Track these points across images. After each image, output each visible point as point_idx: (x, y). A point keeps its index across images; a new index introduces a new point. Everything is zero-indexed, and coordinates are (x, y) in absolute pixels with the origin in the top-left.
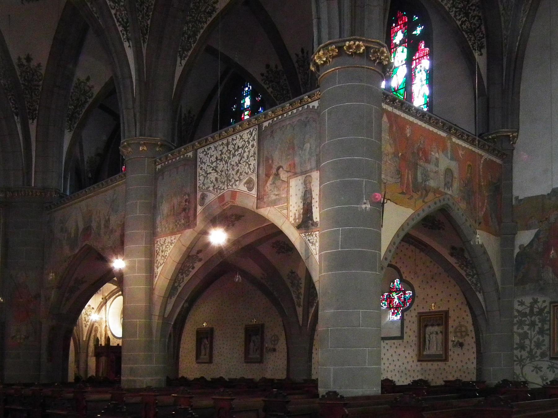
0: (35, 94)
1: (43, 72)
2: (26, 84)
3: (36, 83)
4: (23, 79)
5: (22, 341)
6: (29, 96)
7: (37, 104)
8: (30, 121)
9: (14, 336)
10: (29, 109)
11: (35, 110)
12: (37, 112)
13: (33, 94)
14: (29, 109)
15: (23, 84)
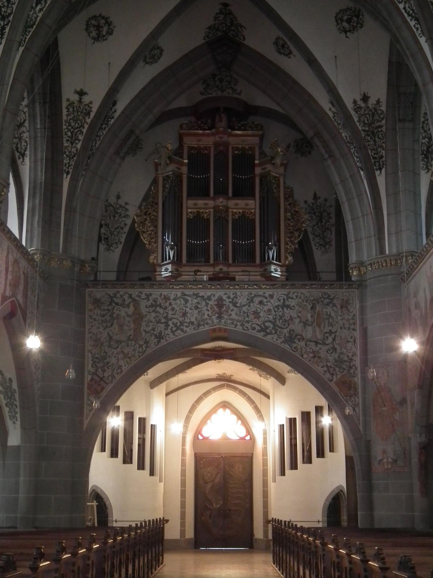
0: (379, 138)
1: (384, 108)
2: (367, 129)
3: (379, 124)
4: (362, 124)
5: (389, 466)
6: (372, 143)
7: (383, 149)
8: (377, 173)
9: (381, 460)
10: (374, 158)
11: (382, 157)
12: (384, 159)
13: (377, 139)
14: (374, 158)
15: (363, 130)
